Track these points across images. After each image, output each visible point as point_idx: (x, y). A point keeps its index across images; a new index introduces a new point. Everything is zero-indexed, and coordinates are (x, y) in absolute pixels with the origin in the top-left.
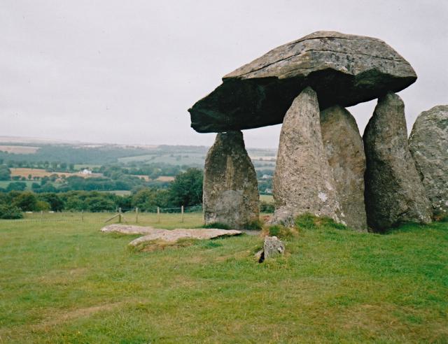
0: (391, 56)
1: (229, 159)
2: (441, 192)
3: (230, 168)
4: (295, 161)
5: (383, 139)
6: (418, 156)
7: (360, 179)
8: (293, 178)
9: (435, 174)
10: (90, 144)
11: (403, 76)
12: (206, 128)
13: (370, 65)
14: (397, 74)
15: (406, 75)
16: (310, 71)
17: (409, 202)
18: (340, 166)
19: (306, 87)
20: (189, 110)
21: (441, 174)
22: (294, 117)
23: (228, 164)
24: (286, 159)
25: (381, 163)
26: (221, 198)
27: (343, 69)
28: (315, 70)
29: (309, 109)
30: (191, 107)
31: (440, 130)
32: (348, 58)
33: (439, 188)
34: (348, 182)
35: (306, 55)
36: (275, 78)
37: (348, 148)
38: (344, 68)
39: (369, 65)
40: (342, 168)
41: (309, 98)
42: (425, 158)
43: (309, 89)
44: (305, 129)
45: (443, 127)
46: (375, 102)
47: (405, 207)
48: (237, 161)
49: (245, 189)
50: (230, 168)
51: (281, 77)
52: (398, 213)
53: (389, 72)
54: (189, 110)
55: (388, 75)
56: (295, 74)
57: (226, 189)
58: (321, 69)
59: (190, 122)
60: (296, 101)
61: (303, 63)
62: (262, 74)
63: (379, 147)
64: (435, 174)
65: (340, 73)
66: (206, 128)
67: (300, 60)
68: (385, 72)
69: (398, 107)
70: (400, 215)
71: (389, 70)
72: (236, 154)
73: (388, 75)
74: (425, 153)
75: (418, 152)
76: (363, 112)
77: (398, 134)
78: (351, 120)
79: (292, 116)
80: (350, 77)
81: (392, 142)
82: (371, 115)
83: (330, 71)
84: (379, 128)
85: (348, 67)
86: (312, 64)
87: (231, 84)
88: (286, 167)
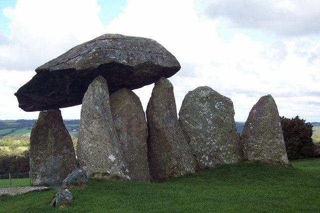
0: (161, 51)
1: (50, 131)
3: (51, 139)
4: (91, 132)
6: (186, 124)
8: (90, 145)
12: (32, 107)
13: (145, 58)
14: (165, 65)
15: (172, 66)
19: (98, 75)
20: (15, 94)
23: (49, 136)
25: (158, 130)
26: (45, 162)
36: (73, 70)
38: (124, 61)
39: (144, 59)
41: (100, 84)
43: (101, 77)
44: (97, 108)
46: (153, 85)
47: (175, 163)
48: (57, 133)
49: (64, 154)
50: (51, 139)
51: (78, 69)
54: (15, 94)
55: (158, 65)
57: (48, 155)
58: (107, 62)
60: (90, 87)
62: (65, 67)
65: (122, 66)
66: (32, 107)
67: (91, 56)
68: (156, 64)
71: (159, 62)
73: (158, 66)
76: (144, 94)
78: (137, 100)
82: (151, 96)
83: (114, 64)
85: (128, 60)
87: (43, 74)
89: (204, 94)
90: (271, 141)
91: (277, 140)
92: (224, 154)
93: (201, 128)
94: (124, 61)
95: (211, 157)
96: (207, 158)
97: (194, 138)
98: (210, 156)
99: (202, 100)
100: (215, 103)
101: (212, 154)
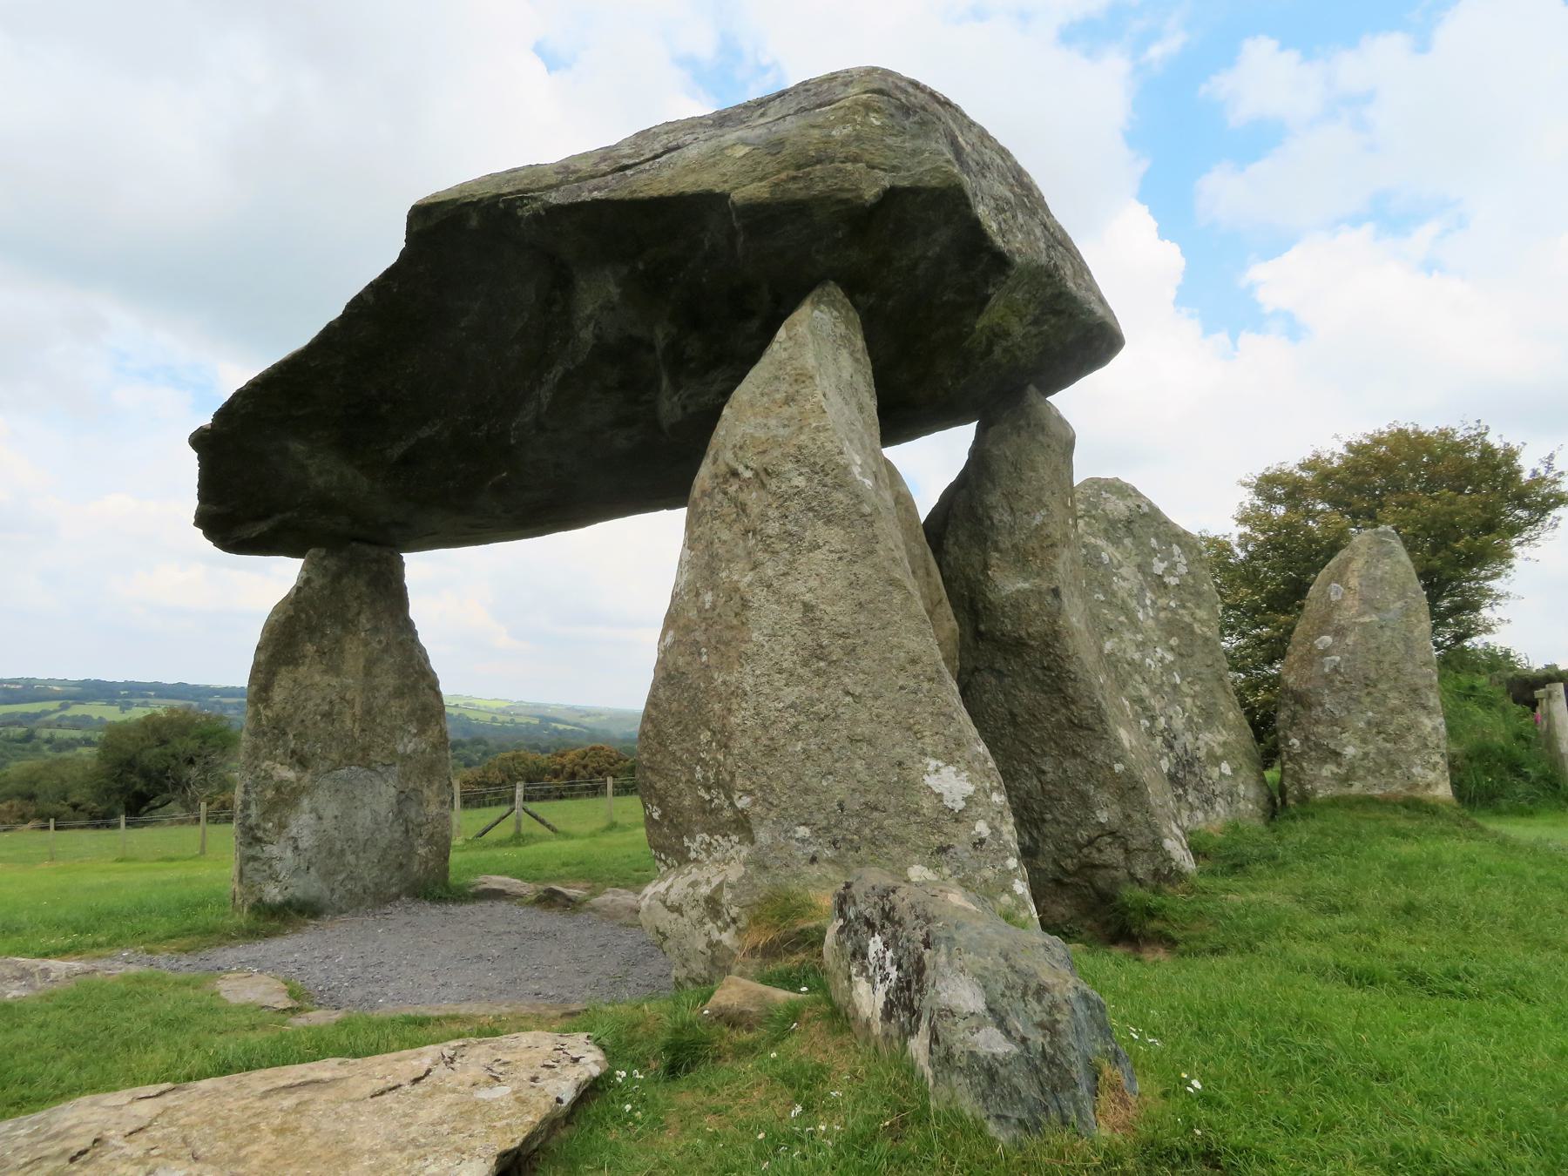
5: (1022, 560)
8: (791, 694)
12: (263, 527)
16: (886, 181)
21: (1145, 691)
22: (789, 400)
24: (759, 596)
25: (1017, 646)
30: (206, 420)
35: (868, 107)
41: (841, 329)
43: (839, 293)
52: (1082, 835)
56: (821, 181)
59: (189, 501)
61: (858, 138)
63: (1009, 584)
66: (263, 527)
67: (844, 121)
70: (1091, 842)
72: (376, 630)
79: (779, 396)
80: (1001, 261)
81: (1059, 565)
84: (1002, 516)
88: (755, 635)
89: (1117, 507)
90: (1401, 720)
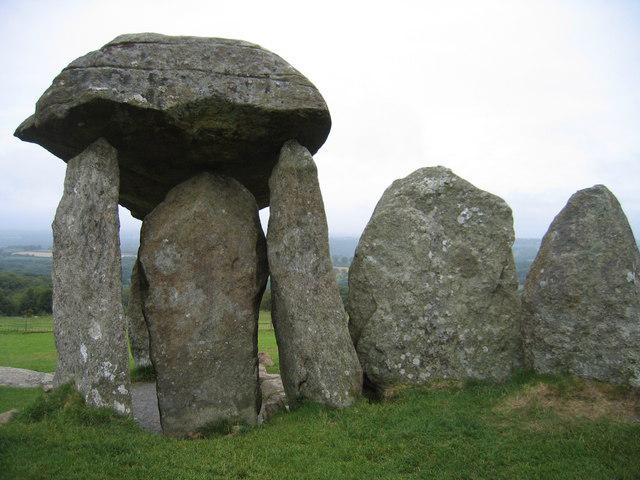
0: (266, 70)
2: (406, 337)
6: (369, 265)
7: (245, 312)
9: (397, 301)
10: (32, 248)
11: (283, 107)
13: (205, 89)
16: (66, 107)
17: (307, 361)
18: (198, 287)
27: (139, 98)
28: (75, 105)
29: (93, 180)
31: (419, 215)
32: (151, 79)
33: (403, 331)
34: (216, 317)
37: (216, 253)
39: (201, 89)
40: (200, 291)
42: (384, 269)
43: (102, 143)
45: (427, 210)
53: (250, 102)
55: (250, 107)
58: (83, 101)
64: (397, 301)
65: (131, 109)
69: (299, 171)
71: (255, 98)
74: (384, 259)
75: (370, 258)
77: (299, 224)
85: (149, 95)
86: (70, 93)
89: (431, 185)
91: (620, 325)
92: (470, 350)
93: (407, 277)
94: (139, 97)
95: (427, 358)
96: (417, 362)
97: (387, 305)
98: (426, 355)
99: (424, 202)
100: (458, 212)
101: (431, 351)
